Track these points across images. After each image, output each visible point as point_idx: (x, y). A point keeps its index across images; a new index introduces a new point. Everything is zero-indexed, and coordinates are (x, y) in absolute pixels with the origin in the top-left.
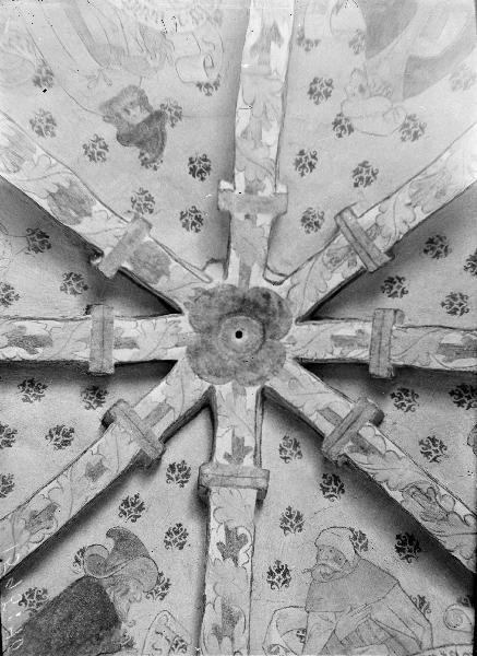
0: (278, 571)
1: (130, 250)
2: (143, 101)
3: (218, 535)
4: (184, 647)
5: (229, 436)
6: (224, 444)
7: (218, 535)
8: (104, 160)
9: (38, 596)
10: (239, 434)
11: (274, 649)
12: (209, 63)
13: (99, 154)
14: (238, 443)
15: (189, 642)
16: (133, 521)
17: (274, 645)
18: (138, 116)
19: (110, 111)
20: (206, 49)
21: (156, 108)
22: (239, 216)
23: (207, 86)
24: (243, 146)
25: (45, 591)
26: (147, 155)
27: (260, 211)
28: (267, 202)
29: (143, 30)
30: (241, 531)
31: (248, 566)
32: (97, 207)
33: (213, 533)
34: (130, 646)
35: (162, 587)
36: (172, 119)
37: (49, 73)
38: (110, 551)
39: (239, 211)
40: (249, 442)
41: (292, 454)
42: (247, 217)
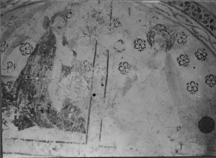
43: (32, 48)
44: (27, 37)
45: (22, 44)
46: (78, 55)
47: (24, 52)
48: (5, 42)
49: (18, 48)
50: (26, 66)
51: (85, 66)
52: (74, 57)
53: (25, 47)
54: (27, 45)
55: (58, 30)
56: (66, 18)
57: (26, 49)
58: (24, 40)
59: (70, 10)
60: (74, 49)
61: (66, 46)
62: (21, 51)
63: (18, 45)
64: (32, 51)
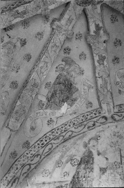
0: (115, 59)
3: (96, 58)
4: (93, 87)
5: (94, 24)
6: (93, 28)
7: (96, 58)
9: (49, 84)
10: (97, 23)
11: (118, 83)
14: (97, 27)
15: (93, 86)
16: (68, 54)
17: (118, 82)
25: (50, 82)
30: (103, 55)
31: (107, 66)
33: (95, 58)
34: (78, 90)
35: (82, 72)
38: (64, 65)
40: (101, 25)
41: (115, 21)
43: (78, 161)
44: (75, 155)
45: (72, 160)
46: (109, 160)
47: (74, 165)
48: (61, 161)
49: (69, 163)
50: (76, 172)
51: (116, 165)
52: (107, 161)
53: (74, 161)
54: (75, 160)
55: (93, 148)
56: (97, 140)
57: (74, 162)
58: (72, 157)
59: (99, 135)
60: (106, 156)
61: (100, 156)
62: (72, 164)
63: (69, 161)
64: (78, 163)
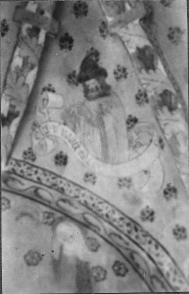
1: (123, 16)
2: (86, 91)
8: (118, 66)
12: (45, 102)
13: (120, 70)
18: (92, 83)
19: (105, 91)
20: (45, 111)
21: (80, 87)
22: (48, 15)
23: (49, 90)
24: (33, 60)
26: (94, 58)
27: (33, 14)
28: (28, 20)
29: (74, 129)
32: (132, 51)
36: (74, 76)
37: (128, 123)
39: (47, 18)
42: (42, 13)
